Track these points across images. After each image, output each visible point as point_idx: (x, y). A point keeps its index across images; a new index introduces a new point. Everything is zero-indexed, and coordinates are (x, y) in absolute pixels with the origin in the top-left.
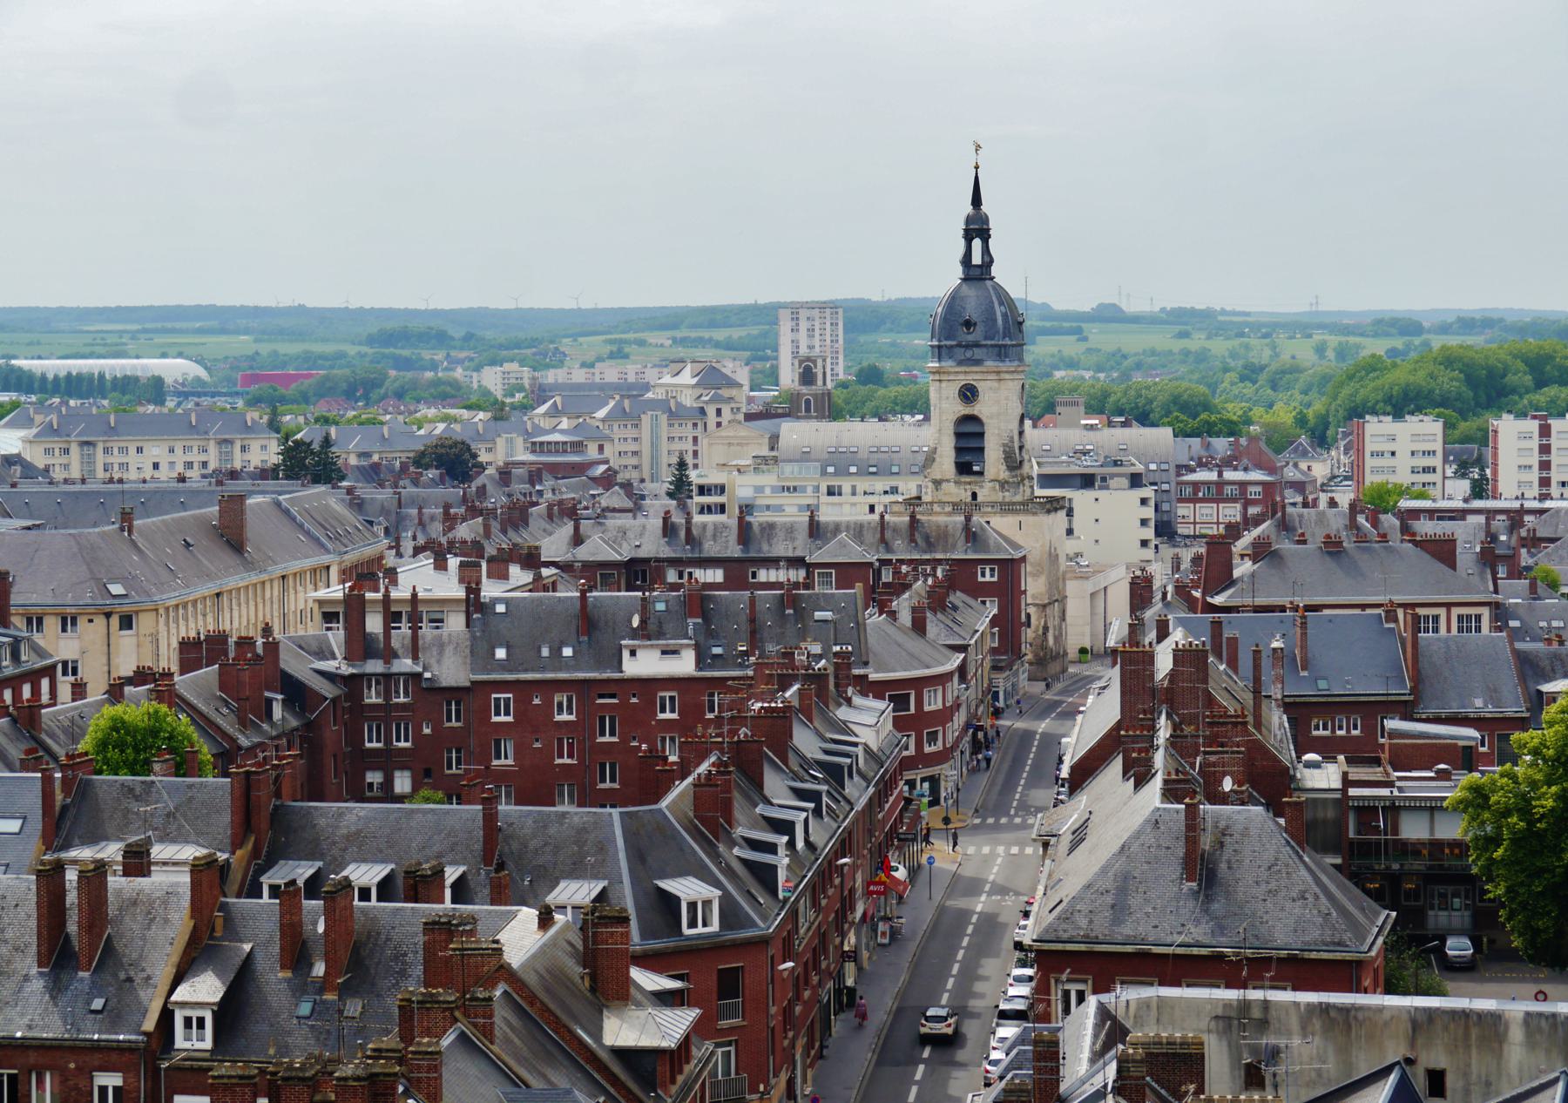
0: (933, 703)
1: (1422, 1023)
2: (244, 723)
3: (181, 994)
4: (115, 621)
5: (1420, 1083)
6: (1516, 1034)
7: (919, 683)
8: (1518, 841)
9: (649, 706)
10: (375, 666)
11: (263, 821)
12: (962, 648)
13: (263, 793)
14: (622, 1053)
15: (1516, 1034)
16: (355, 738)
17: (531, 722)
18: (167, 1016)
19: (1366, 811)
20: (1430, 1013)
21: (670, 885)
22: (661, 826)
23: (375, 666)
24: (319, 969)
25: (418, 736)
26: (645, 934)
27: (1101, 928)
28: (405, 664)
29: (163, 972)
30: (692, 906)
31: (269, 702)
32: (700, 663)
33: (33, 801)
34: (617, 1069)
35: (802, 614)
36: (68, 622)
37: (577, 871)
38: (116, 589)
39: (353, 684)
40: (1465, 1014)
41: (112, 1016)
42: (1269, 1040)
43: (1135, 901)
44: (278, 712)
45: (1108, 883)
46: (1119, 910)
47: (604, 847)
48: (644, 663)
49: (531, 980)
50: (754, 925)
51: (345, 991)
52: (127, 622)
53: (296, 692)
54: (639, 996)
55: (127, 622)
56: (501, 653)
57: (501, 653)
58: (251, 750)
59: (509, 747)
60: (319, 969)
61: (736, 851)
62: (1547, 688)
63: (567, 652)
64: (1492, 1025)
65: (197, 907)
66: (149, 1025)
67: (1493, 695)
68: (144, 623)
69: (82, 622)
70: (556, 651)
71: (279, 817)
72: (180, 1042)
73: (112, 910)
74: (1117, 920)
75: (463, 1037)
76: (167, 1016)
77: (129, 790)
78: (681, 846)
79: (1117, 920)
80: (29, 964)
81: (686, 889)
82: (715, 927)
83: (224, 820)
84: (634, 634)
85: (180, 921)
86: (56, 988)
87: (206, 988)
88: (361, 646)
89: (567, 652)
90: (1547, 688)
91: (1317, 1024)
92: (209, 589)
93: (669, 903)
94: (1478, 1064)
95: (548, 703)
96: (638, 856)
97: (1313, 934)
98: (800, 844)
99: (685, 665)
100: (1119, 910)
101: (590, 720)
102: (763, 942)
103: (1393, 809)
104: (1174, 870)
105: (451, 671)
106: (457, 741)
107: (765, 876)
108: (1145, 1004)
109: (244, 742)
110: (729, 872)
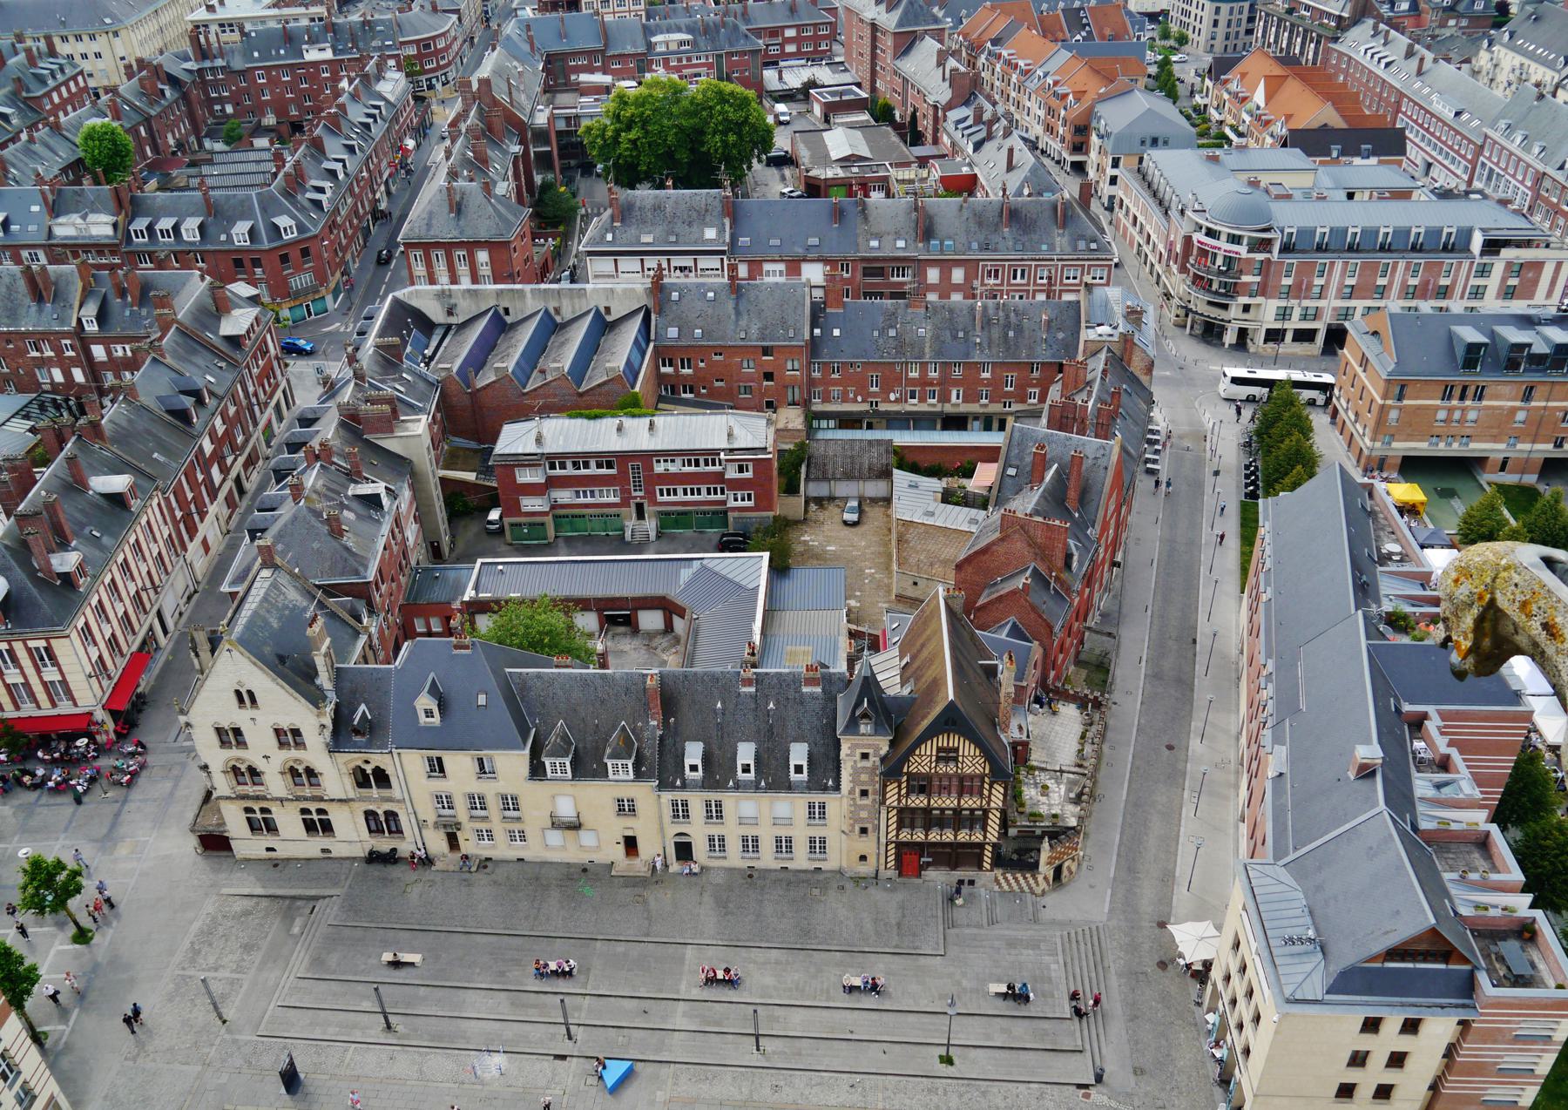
0: (441, 44)
1: (499, 293)
2: (151, 103)
3: (82, 313)
4: (111, 35)
5: (502, 312)
6: (529, 295)
7: (434, 38)
8: (601, 148)
9: (318, 72)
10: (207, 64)
11: (126, 202)
12: (457, 11)
13: (123, 195)
14: (228, 339)
15: (529, 295)
16: (207, 94)
17: (273, 82)
18: (79, 321)
19: (568, 119)
20: (502, 290)
21: (276, 220)
22: (272, 197)
23: (207, 64)
24: (129, 299)
25: (231, 91)
26: (270, 241)
27: (423, 233)
28: (219, 62)
29: (77, 304)
30: (285, 229)
31: (162, 91)
32: (335, 53)
33: (40, 197)
34: (224, 347)
35: (372, 29)
36: (92, 37)
37: (243, 217)
38: (108, 21)
39: (199, 70)
40: (512, 290)
41: (61, 320)
42: (453, 301)
43: (434, 222)
44: (168, 93)
45: (425, 216)
46: (429, 226)
47: (251, 207)
48: (312, 55)
49: (187, 322)
50: (309, 230)
51: (141, 305)
52: (116, 34)
53: (173, 81)
54: (240, 302)
55: (116, 34)
56: (256, 54)
57: (256, 54)
58: (159, 116)
59: (267, 92)
60: (129, 299)
61: (308, 195)
62: (654, 39)
63: (282, 52)
64: (521, 293)
65: (82, 279)
66: (74, 323)
67: (634, 45)
68: (122, 33)
69: (97, 37)
70: (278, 52)
71: (133, 200)
72: (87, 328)
73: (53, 279)
74: (428, 230)
75: (154, 359)
76: (79, 321)
77: (75, 192)
78: (281, 204)
79: (428, 230)
80: (28, 301)
81: (283, 221)
82: (296, 234)
83: (112, 205)
84: (306, 43)
85: (80, 285)
86: (40, 311)
87: (91, 310)
88: (203, 53)
89: (282, 52)
90: (654, 39)
91: (467, 295)
92: (152, 9)
93: (276, 227)
94: (518, 304)
95: (278, 74)
96: (264, 210)
97: (493, 232)
98: (341, 176)
99: (328, 55)
100: (429, 226)
101: (297, 79)
102: (316, 237)
103: (577, 117)
104: (446, 209)
105: (238, 64)
106: (246, 91)
107: (317, 204)
108: (411, 293)
109: (153, 113)
110: (302, 209)
